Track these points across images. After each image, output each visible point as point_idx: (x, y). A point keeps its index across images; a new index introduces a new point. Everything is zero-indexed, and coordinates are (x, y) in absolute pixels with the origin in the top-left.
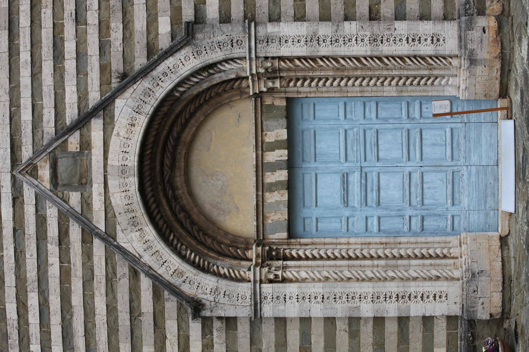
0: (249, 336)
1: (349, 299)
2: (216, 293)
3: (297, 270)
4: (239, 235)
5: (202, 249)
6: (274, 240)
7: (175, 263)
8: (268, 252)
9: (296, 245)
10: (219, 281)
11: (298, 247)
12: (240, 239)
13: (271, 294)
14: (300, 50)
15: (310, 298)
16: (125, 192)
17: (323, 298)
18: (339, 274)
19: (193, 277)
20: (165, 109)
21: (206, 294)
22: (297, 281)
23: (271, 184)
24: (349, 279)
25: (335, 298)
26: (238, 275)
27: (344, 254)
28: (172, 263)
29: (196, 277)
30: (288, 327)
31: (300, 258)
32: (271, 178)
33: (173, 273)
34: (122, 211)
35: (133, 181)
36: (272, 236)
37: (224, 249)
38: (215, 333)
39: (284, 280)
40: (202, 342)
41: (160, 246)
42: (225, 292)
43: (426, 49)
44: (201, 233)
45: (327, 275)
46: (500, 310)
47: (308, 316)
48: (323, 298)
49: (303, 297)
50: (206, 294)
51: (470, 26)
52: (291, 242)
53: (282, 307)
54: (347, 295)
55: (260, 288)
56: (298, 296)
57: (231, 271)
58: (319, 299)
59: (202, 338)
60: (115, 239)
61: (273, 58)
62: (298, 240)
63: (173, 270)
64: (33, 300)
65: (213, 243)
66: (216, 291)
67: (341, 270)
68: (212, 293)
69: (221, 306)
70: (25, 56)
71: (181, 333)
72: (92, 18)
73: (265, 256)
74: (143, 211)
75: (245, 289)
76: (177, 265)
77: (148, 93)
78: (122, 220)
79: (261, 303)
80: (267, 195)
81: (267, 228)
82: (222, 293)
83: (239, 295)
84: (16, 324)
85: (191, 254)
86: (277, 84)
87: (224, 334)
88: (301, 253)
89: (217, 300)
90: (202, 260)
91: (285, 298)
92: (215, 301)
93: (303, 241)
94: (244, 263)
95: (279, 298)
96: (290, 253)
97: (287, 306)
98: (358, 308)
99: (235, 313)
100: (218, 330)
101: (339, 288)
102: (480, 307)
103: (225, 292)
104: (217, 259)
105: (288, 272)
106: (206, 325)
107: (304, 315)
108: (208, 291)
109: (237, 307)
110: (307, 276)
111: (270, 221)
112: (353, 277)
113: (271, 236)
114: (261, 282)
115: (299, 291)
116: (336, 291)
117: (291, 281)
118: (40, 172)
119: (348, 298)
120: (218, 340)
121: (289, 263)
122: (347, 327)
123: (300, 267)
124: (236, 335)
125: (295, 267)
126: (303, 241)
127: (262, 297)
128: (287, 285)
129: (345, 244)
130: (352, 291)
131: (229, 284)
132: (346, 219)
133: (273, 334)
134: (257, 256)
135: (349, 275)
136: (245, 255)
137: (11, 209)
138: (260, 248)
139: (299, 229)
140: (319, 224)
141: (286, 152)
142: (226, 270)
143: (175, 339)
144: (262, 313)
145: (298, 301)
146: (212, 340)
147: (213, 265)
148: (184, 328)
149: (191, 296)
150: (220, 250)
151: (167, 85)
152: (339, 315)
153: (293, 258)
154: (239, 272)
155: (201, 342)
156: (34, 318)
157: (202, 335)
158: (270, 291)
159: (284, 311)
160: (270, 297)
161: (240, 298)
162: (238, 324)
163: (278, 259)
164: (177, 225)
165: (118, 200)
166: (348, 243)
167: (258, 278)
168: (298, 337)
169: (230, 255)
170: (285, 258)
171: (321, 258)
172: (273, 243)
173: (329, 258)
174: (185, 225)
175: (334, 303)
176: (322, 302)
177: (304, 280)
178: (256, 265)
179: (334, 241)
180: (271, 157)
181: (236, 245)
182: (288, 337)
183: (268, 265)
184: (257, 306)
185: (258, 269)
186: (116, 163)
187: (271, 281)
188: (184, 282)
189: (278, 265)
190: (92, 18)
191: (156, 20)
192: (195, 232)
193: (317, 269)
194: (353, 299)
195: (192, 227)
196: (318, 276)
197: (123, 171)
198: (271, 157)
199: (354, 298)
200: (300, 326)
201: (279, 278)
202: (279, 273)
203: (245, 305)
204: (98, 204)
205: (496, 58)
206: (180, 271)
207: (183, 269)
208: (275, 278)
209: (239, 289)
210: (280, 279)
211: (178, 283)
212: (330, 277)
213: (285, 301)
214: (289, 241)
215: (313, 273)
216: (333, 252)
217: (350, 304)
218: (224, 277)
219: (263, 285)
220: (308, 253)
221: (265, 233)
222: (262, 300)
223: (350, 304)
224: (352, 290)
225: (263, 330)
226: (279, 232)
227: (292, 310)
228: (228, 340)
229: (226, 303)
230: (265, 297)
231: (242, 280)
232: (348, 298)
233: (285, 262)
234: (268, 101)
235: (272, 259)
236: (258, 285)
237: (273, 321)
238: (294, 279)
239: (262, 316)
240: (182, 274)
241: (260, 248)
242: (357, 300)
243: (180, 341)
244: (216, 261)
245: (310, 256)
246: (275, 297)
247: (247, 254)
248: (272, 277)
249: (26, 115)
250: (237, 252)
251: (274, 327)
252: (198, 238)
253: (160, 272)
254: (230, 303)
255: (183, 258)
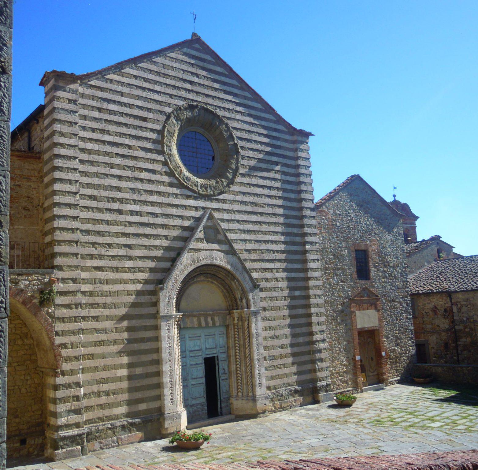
14: (254, 331)
16: (204, 258)
20: (230, 276)
23: (200, 319)
32: (202, 319)
34: (198, 256)
35: (209, 262)
38: (149, 297)
41: (186, 273)
43: (257, 382)
46: (169, 432)
51: (266, 398)
60: (188, 252)
61: (248, 320)
64: (158, 210)
70: (245, 217)
72: (257, 246)
74: (199, 265)
77: (237, 270)
78: (195, 255)
80: (196, 318)
84: (148, 200)
86: (236, 322)
100: (150, 298)
102: (170, 422)
111: (187, 320)
118: (210, 221)
137: (193, 205)
141: (212, 326)
151: (240, 277)
156: (150, 209)
165: (202, 254)
168: (149, 336)
180: (209, 319)
186: (214, 255)
190: (257, 246)
191: (256, 272)
197: (212, 258)
198: (209, 319)
204: (200, 245)
205: (257, 411)
227: (164, 333)
234: (228, 317)
240: (176, 282)
249: (226, 216)
253: (176, 272)
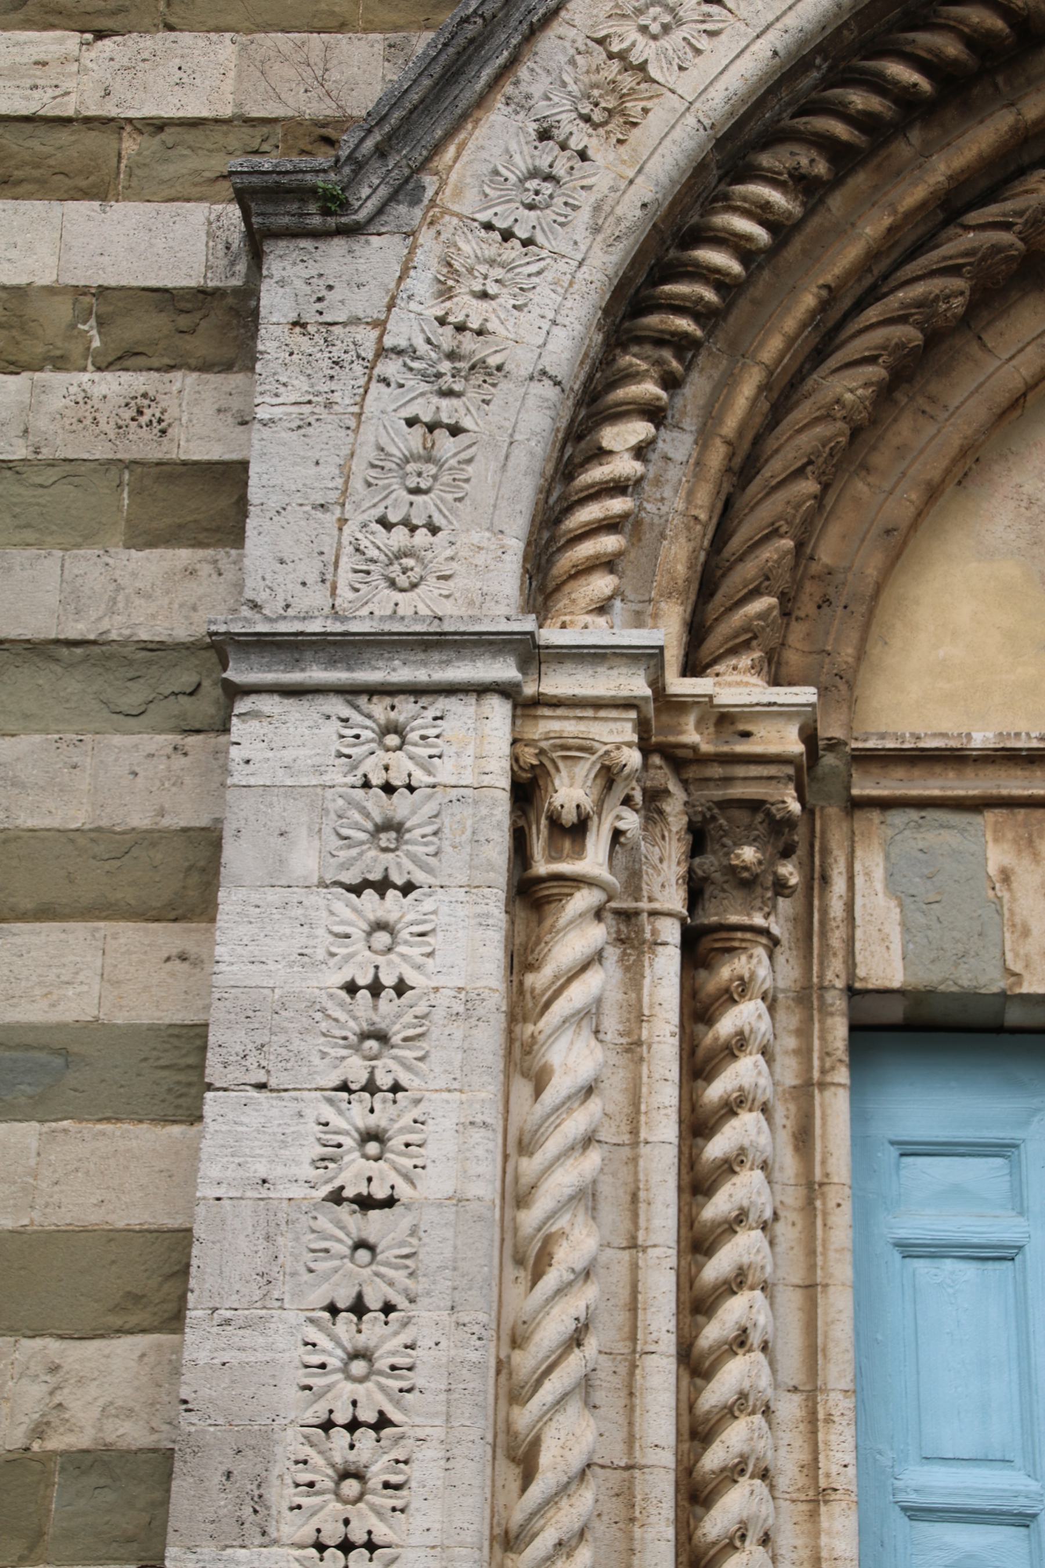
0: (75, 630)
1: (340, 1437)
2: (445, 366)
3: (611, 1024)
4: (875, 650)
5: (790, 324)
6: (839, 885)
7: (702, 69)
8: (755, 806)
9: (804, 1053)
10: (547, 390)
11: (789, 1072)
12: (854, 636)
13: (420, 777)
15: (371, 1087)
17: (366, 1203)
18: (574, 1365)
19: (586, 201)
21: (445, 293)
22: (522, 1007)
24: (525, 1460)
25: (359, 1308)
26: (587, 549)
27: (734, 1439)
28: (704, 43)
29: (584, 217)
30: (128, 934)
31: (698, 1065)
33: (622, 56)
36: (879, 874)
37: (781, 497)
38: (113, 386)
39: (531, 896)
40: (50, 290)
42: (455, 430)
44: (910, 334)
45: (568, 1256)
47: (214, 1072)
48: (366, 1203)
49: (383, 1038)
50: (445, 293)
52: (825, 1011)
53: (305, 860)
54: (383, 1422)
55: (481, 690)
56: (401, 988)
57: (618, 505)
58: (354, 1173)
59: (80, 291)
62: (842, 1075)
63: (644, 50)
65: (827, 417)
66: (464, 364)
67: (599, 1396)
68: (446, 338)
69: (344, 400)
71: (130, 145)
73: (727, 781)
75: (479, 577)
76: (687, 85)
79: (350, 692)
81: (944, 835)
82: (448, 410)
83: (422, 536)
85: (761, 212)
87: (101, 451)
88: (743, 1073)
89: (390, 368)
90: (709, 295)
91: (382, 886)
92: (382, 352)
93: (836, 1108)
94: (667, 632)
95: (386, 839)
96: (743, 988)
97: (317, 898)
98: (253, 1521)
99: (274, 502)
100: (138, 407)
101: (440, 1345)
103: (455, 430)
104: (704, 437)
105: (596, 934)
106: (183, 321)
107: (225, 1039)
108: (465, 307)
109: (330, 519)
110: (558, 1087)
111: (997, 856)
112: (537, 1490)
113: (872, 865)
114: (526, 706)
115: (443, 999)
116: (427, 1321)
117: (521, 960)
119: (353, 1426)
120: (56, 402)
121: (666, 966)
122: (83, 1441)
123: (634, 1048)
124: (88, 536)
125: (637, 1016)
126: (836, 1108)
127: (406, 709)
128: (494, 902)
129: (812, 1467)
130: (414, 1472)
131: (521, 459)
132: (1018, 1504)
133: (75, 815)
134: (725, 720)
135: (555, 1460)
136: (734, 651)
138: (789, 742)
139: (931, 1104)
140: (969, 1271)
142: (624, 466)
143: (81, 98)
144: (268, 704)
145: (352, 988)
146: (60, 363)
147: (671, 382)
148: (168, 171)
149: (430, 182)
150: (775, 468)
152: (200, 1343)
153: (698, 1011)
154: (609, 564)
155: (46, 279)
157: (103, 291)
158: (445, 772)
159: (277, 876)
160: (402, 766)
161: (399, 537)
162: (184, 555)
163: (696, 891)
164: (980, 139)
166: (818, 1496)
167: (559, 683)
169: (736, 543)
170: (699, 947)
171: (698, 1243)
172: (817, 880)
173: (697, 1304)
174: (973, 217)
175: (320, 1296)
176: (336, 1197)
177: (522, 1062)
178: (666, 703)
179: (838, 1372)
181: (806, 606)
182: (49, 931)
183: (654, 797)
184: (332, 663)
185: (637, 685)
187: (526, 790)
188: (544, 135)
189: (651, 882)
192: (918, 290)
193: (611, 1191)
194: (345, 1475)
195: (954, 271)
196: (565, 1179)
199: (351, 1487)
200: (132, 1032)
201: (553, 857)
202: (593, 859)
203: (345, 576)
206: (634, 107)
207: (654, 124)
208: (555, 822)
209: (477, 537)
210: (542, 867)
211: (537, 90)
212: (551, 1280)
213: (357, 890)
214: (838, 1002)
215: (588, 1141)
216: (755, 1338)
217: (292, 1443)
218: (577, 442)
219: (498, 712)
220: (741, 1131)
221: (898, 818)
222: (379, 708)
223: (292, 1443)
224: (426, 1469)
225: (117, 739)
226: (906, 927)
227: (276, 942)
228: (50, 476)
229: (369, 433)
230: (396, 729)
231: (542, 587)
232: (353, 1426)
233: (671, 932)
235: (699, 837)
236: (503, 670)
237: (187, 813)
238: (538, 980)
239: (242, 706)
240: (613, 113)
241: (789, 742)
242: (328, 1516)
243: (64, 136)
244: (690, 423)
245: (717, 1148)
246: (401, 805)
247: (745, 661)
248: (570, 791)
250: (755, 593)
251: (141, 820)
252: (872, 314)
254: (359, 467)
255: (733, 152)
